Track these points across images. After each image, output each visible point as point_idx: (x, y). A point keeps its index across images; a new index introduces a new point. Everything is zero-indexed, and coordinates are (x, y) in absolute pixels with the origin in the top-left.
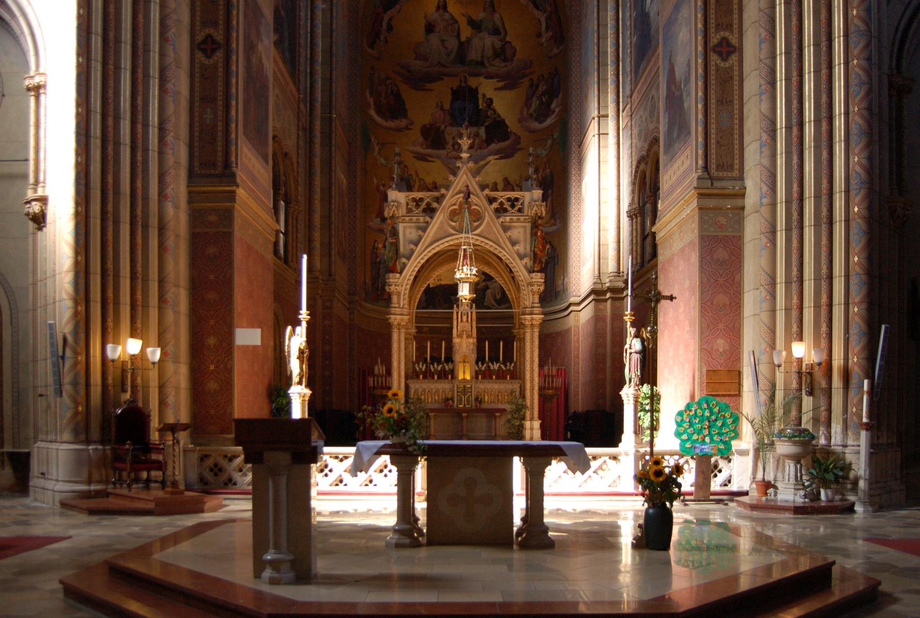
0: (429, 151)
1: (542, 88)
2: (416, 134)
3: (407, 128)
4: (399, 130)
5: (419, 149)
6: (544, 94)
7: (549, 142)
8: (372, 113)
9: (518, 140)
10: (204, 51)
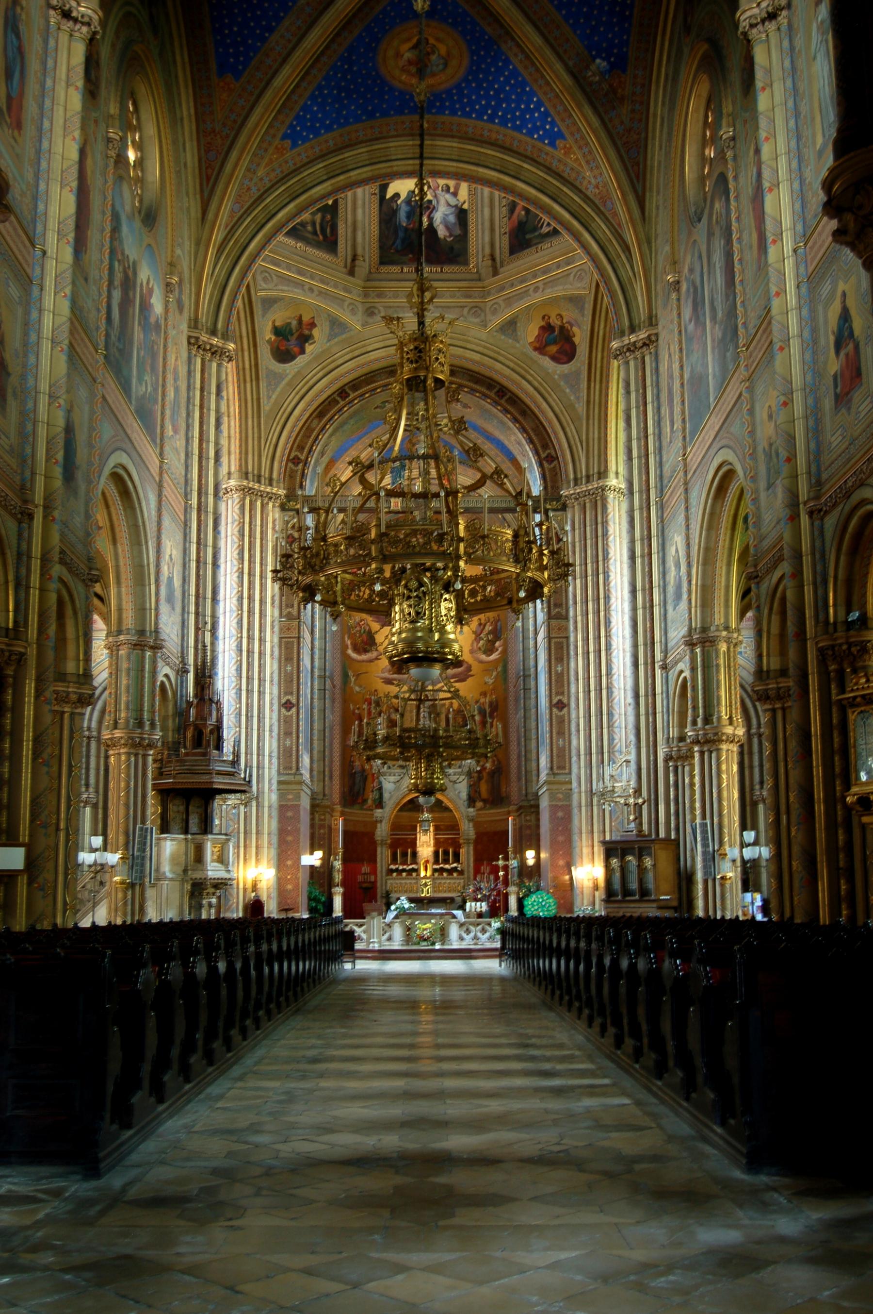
0: (395, 676)
1: (489, 628)
2: (384, 663)
3: (377, 659)
4: (371, 661)
5: (386, 675)
6: (490, 633)
7: (495, 674)
8: (350, 652)
9: (469, 668)
10: (286, 708)
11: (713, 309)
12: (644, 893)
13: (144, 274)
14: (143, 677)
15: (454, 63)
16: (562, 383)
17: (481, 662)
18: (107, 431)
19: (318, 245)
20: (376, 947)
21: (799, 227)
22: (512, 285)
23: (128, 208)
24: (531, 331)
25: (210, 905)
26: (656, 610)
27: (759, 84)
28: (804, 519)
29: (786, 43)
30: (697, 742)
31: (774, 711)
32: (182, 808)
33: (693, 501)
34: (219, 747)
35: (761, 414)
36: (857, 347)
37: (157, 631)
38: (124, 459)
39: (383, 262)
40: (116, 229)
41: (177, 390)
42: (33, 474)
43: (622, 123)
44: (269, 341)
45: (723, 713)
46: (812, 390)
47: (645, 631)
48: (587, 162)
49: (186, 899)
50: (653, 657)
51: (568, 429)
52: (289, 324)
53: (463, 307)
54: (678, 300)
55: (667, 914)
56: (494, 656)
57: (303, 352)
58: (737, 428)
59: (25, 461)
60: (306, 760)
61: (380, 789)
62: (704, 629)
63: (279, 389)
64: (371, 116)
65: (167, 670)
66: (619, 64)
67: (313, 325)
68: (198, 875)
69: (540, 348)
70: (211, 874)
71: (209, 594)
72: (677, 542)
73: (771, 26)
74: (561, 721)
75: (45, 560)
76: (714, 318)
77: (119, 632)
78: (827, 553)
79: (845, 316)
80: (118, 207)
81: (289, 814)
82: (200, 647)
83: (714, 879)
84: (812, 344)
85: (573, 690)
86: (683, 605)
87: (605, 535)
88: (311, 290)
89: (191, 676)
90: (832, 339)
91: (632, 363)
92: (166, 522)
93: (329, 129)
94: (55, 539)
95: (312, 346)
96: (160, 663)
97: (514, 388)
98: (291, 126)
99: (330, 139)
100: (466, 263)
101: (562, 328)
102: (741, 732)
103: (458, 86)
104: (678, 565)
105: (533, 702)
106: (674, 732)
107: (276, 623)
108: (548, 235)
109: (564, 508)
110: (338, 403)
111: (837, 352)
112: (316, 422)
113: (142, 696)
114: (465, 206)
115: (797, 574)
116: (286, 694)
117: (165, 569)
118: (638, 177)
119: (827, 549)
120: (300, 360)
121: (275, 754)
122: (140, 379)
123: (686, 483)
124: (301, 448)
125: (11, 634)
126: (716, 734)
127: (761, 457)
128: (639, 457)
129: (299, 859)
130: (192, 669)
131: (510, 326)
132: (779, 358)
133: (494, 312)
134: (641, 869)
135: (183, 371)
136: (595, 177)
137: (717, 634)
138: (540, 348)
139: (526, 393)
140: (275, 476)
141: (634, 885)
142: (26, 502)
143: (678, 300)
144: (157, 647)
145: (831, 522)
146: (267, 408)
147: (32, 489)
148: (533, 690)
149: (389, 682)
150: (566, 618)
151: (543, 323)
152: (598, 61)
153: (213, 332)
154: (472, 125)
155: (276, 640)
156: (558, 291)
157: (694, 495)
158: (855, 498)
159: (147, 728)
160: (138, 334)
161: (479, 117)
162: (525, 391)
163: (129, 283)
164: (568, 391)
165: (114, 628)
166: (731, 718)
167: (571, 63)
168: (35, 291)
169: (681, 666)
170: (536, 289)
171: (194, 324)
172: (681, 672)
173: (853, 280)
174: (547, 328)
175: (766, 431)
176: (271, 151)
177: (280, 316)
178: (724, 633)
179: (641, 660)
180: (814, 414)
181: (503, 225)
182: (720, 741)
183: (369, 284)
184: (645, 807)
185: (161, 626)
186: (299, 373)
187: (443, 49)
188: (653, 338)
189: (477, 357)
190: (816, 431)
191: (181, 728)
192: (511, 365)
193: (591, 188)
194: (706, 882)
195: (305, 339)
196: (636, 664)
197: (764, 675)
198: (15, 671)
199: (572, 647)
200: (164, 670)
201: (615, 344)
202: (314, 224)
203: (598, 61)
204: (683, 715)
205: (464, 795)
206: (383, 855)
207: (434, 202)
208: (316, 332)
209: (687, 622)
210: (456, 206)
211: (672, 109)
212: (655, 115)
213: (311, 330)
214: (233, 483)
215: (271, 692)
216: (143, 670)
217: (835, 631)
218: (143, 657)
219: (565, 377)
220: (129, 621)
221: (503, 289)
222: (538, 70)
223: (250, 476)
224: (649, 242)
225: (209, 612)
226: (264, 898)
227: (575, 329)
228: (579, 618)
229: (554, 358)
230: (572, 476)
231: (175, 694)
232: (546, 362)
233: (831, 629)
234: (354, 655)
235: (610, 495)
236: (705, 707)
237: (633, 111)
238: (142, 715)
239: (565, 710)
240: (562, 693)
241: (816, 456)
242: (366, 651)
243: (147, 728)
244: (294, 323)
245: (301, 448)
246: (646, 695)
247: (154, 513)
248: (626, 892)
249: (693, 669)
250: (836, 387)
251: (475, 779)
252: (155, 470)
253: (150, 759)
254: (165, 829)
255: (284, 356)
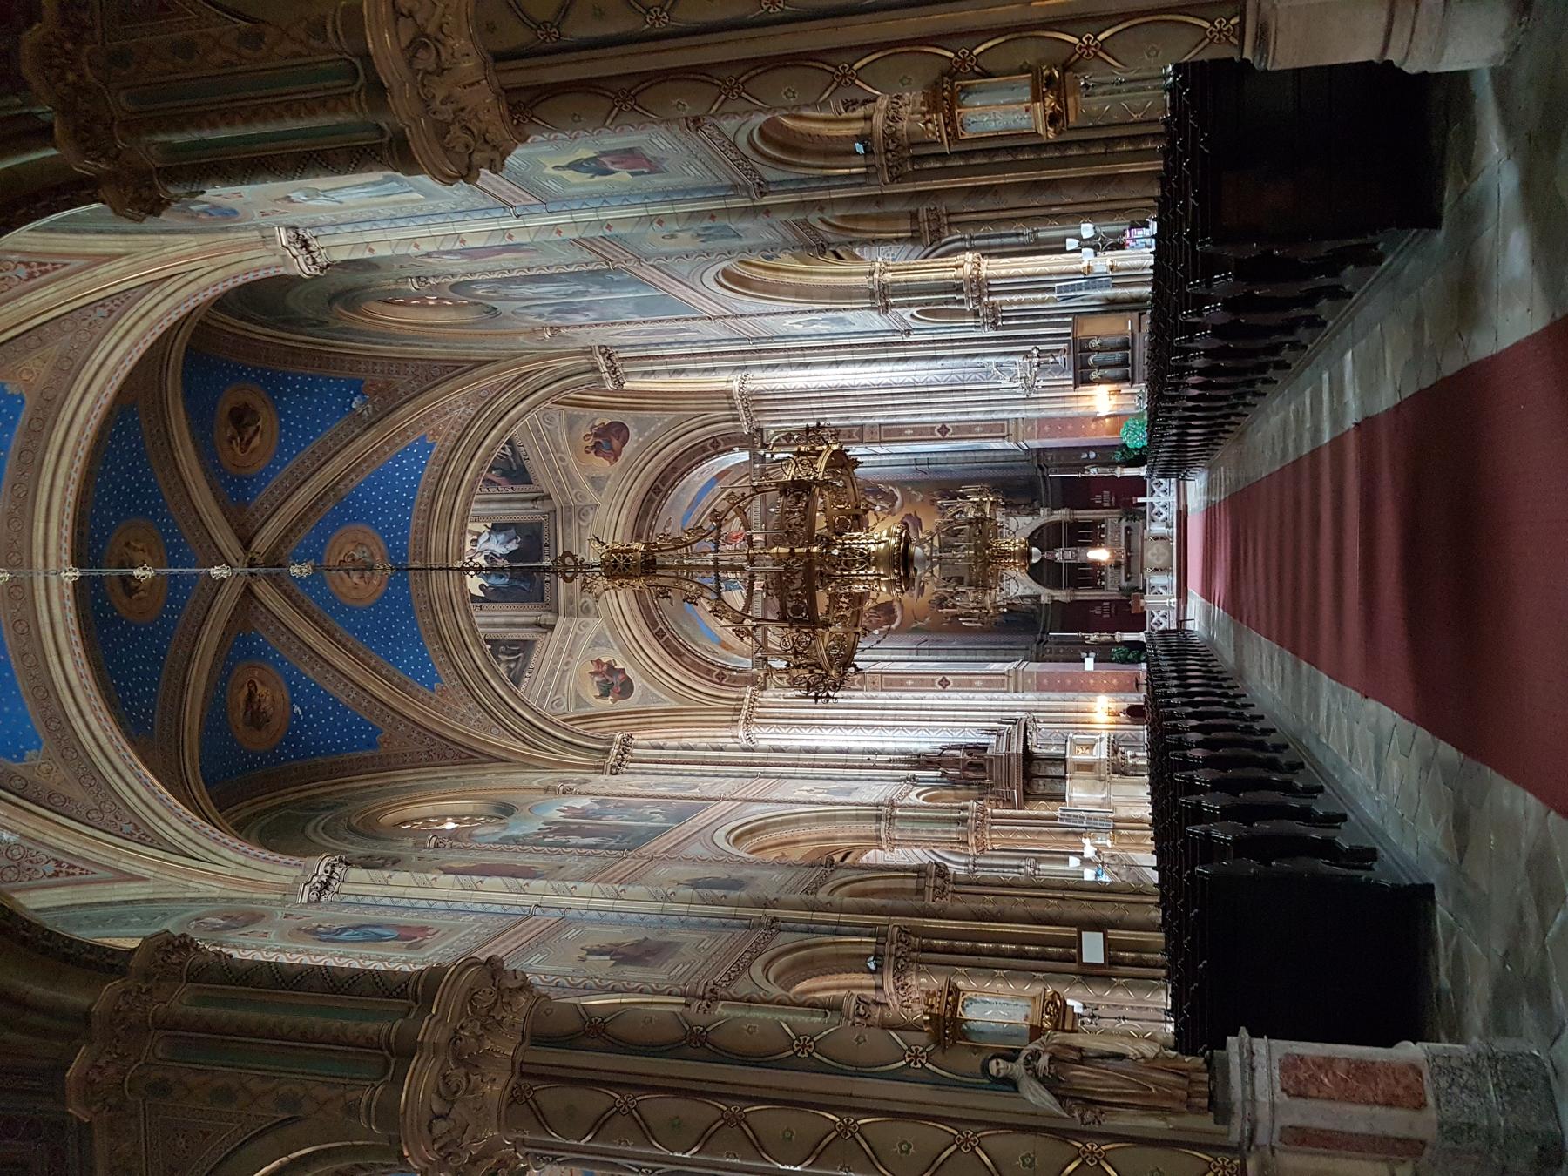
4: (902, 606)
6: (875, 497)
11: (573, 294)
12: (1125, 346)
13: (556, 815)
14: (919, 817)
15: (360, 537)
17: (903, 506)
18: (695, 850)
19: (527, 658)
20: (1175, 600)
21: (498, 213)
22: (559, 481)
23: (497, 829)
24: (600, 464)
25: (1134, 756)
26: (853, 342)
27: (367, 255)
28: (767, 200)
29: (329, 231)
30: (979, 299)
31: (950, 224)
32: (1041, 782)
33: (753, 309)
34: (984, 748)
35: (669, 246)
36: (604, 154)
37: (877, 805)
38: (722, 833)
39: (542, 600)
40: (516, 840)
41: (657, 785)
42: (735, 917)
43: (409, 382)
45: (952, 274)
46: (647, 198)
47: (874, 352)
48: (446, 413)
49: (1128, 779)
50: (898, 343)
51: (688, 428)
53: (580, 526)
54: (568, 327)
55: (1147, 321)
56: (898, 493)
57: (622, 671)
58: (684, 267)
59: (724, 925)
60: (995, 667)
61: (1022, 597)
62: (872, 295)
63: (657, 692)
64: (410, 611)
65: (913, 795)
66: (357, 387)
68: (1105, 768)
69: (616, 455)
70: (1104, 756)
71: (844, 756)
72: (790, 324)
73: (314, 245)
74: (958, 429)
75: (813, 908)
76: (584, 293)
77: (879, 838)
78: (799, 177)
79: (576, 166)
80: (496, 838)
81: (1045, 681)
82: (892, 765)
83: (1113, 277)
84: (605, 199)
85: (929, 419)
86: (848, 315)
87: (784, 392)
88: (567, 664)
89: (917, 773)
90: (597, 178)
91: (626, 370)
92: (776, 795)
93: (423, 649)
94: (796, 897)
96: (906, 801)
97: (652, 478)
98: (422, 683)
99: (433, 648)
100: (541, 523)
101: (596, 435)
102: (969, 256)
103: (382, 533)
104: (813, 322)
105: (940, 456)
106: (970, 321)
107: (868, 694)
108: (512, 450)
109: (760, 430)
111: (613, 172)
112: (685, 659)
113: (937, 818)
114: (490, 525)
115: (820, 205)
116: (933, 685)
117: (820, 797)
118: (458, 367)
119: (792, 177)
120: (630, 672)
121: (989, 695)
122: (650, 819)
123: (736, 316)
124: (709, 672)
125: (882, 940)
126: (972, 281)
127: (711, 244)
128: (713, 361)
129: (1088, 672)
130: (912, 772)
131: (597, 483)
132: (618, 230)
133: (583, 497)
134: (1102, 349)
135: (641, 779)
136: (459, 407)
137: (876, 283)
139: (656, 467)
140: (735, 696)
141: (1118, 355)
142: (760, 924)
143: (568, 327)
144: (892, 805)
145: (771, 174)
146: (674, 703)
147: (750, 918)
148: (928, 456)
149: (922, 590)
150: (862, 426)
152: (354, 406)
153: (607, 752)
154: (416, 522)
155: (884, 694)
156: (563, 440)
157: (747, 309)
158: (748, 152)
159: (967, 814)
160: (609, 820)
161: (410, 513)
162: (653, 468)
163: (563, 829)
165: (874, 843)
166: (957, 267)
167: (357, 431)
168: (570, 914)
169: (907, 317)
170: (562, 460)
171: (599, 769)
172: (912, 316)
173: (543, 160)
174: (597, 449)
175: (686, 241)
176: (444, 701)
177: (591, 691)
178: (876, 276)
179: (902, 355)
180: (668, 195)
181: (505, 491)
182: (978, 276)
183: (561, 611)
184: (1041, 347)
185: (872, 801)
186: (641, 674)
187: (350, 547)
188: (603, 350)
189: (624, 512)
190: (686, 193)
191: (968, 783)
192: (631, 481)
193: (469, 411)
194: (1115, 286)
195: (611, 668)
196: (906, 359)
197: (917, 235)
198: (916, 936)
199: (889, 421)
200: (913, 798)
201: (610, 386)
202: (509, 661)
203: (354, 406)
204: (953, 313)
205: (1028, 519)
206: (1084, 595)
207: (487, 553)
208: (605, 660)
209: (866, 312)
211: (395, 337)
212: (400, 352)
213: (603, 664)
214: (741, 734)
215: (932, 698)
216: (913, 817)
217: (874, 166)
218: (901, 816)
219: (640, 434)
220: (869, 828)
221: (563, 490)
222: (364, 461)
223: (735, 718)
224: (516, 356)
225: (859, 757)
226: (1126, 705)
227: (597, 423)
228: (862, 414)
230: (730, 424)
231: (935, 788)
232: (627, 449)
233: (873, 170)
234: (897, 623)
235: (749, 387)
236: (946, 293)
237: (398, 373)
238: (955, 819)
239: (948, 425)
240: (933, 428)
241: (709, 192)
242: (893, 611)
243: (967, 814)
244: (597, 679)
245: (709, 672)
246: (935, 349)
247: (770, 806)
248: (1124, 363)
249: (910, 304)
250: (643, 173)
251: (1012, 507)
252: (731, 805)
253: (995, 811)
254: (1061, 798)
255: (627, 688)
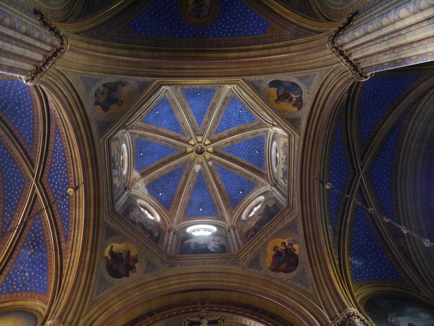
16: (295, 283)
44: (106, 258)
52: (121, 254)
67: (136, 260)
95: (134, 274)
101: (287, 250)
110: (146, 318)
120: (124, 279)
138: (275, 268)
151: (274, 253)
164: (299, 285)
208: (137, 265)
210: (219, 244)
229: (286, 271)
232: (282, 275)
235: (357, 321)
244: (125, 255)
